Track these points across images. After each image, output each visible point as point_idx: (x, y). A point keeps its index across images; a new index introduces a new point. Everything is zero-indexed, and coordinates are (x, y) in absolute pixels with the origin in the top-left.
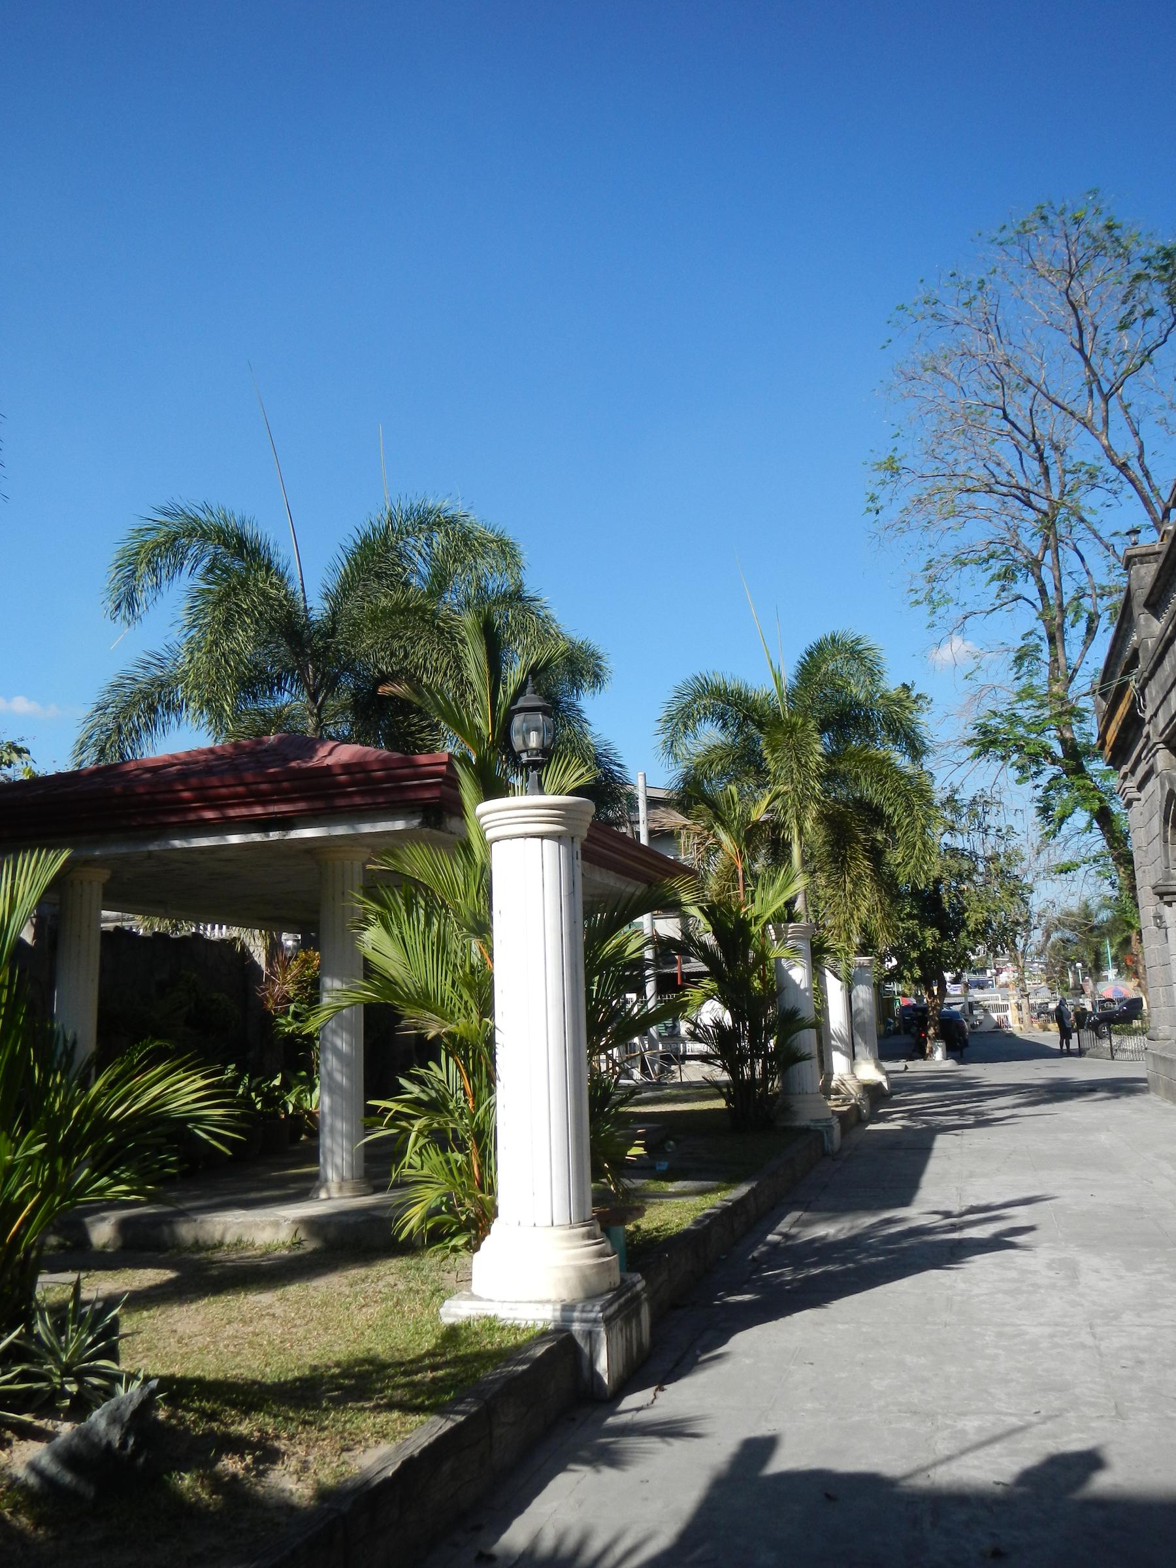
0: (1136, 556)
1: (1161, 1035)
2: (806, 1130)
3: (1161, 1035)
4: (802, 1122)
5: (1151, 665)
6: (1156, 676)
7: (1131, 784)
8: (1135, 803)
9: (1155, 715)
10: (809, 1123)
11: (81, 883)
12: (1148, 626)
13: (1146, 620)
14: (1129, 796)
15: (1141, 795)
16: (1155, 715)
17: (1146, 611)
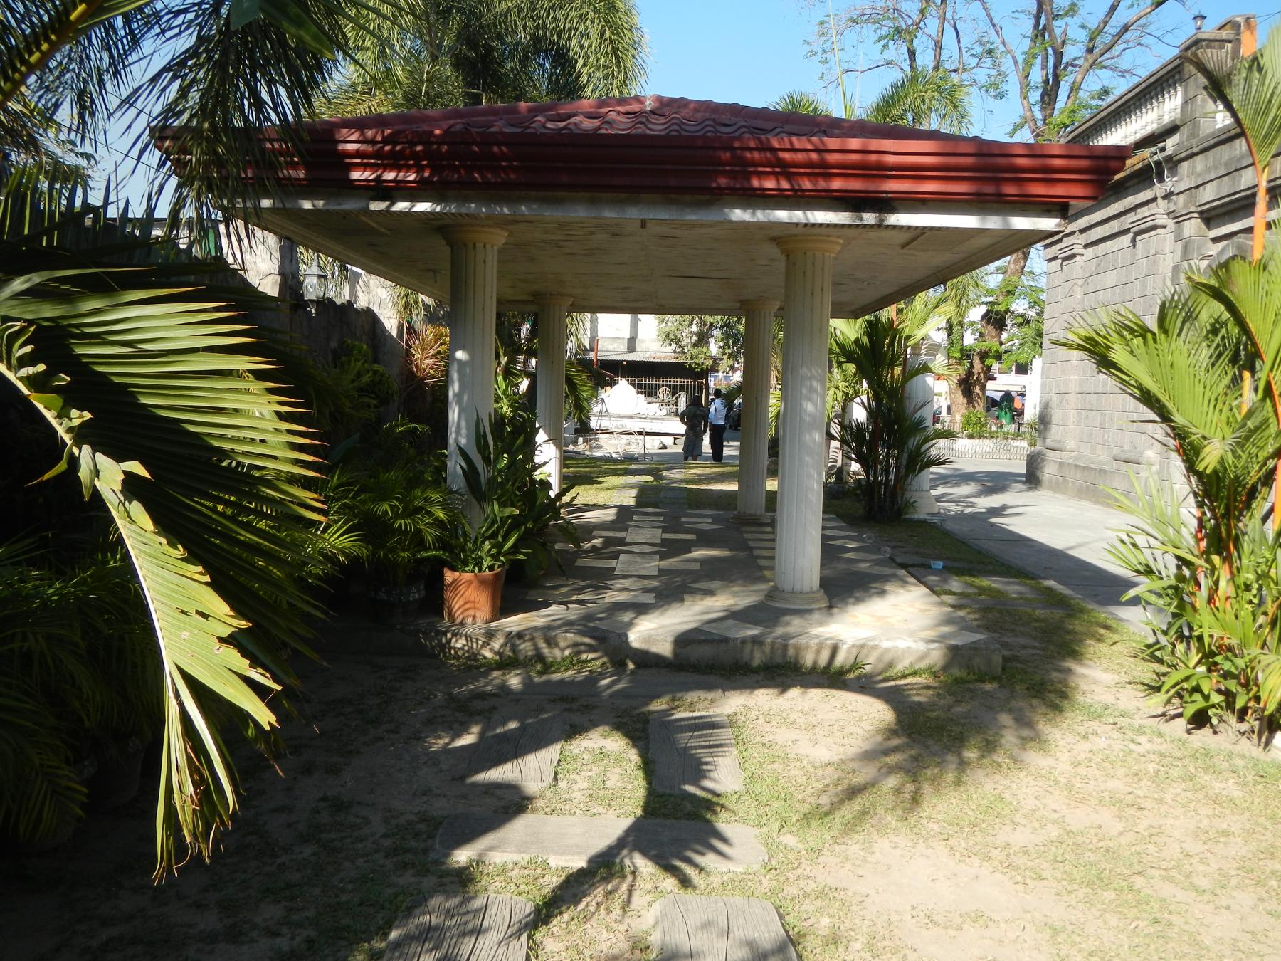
0: (1204, 40)
1: (1068, 448)
2: (923, 523)
3: (1068, 448)
4: (921, 514)
5: (1212, 142)
6: (1210, 153)
7: (1079, 242)
8: (1078, 258)
9: (1197, 187)
10: (926, 516)
11: (474, 247)
12: (1203, 107)
13: (1203, 101)
14: (1075, 251)
15: (1090, 252)
16: (1197, 187)
17: (1204, 93)
